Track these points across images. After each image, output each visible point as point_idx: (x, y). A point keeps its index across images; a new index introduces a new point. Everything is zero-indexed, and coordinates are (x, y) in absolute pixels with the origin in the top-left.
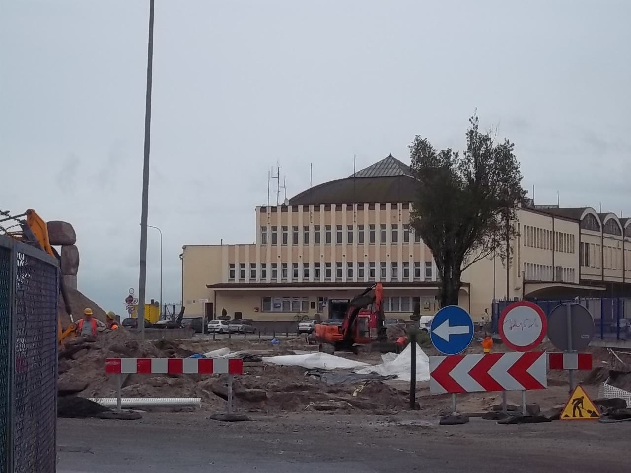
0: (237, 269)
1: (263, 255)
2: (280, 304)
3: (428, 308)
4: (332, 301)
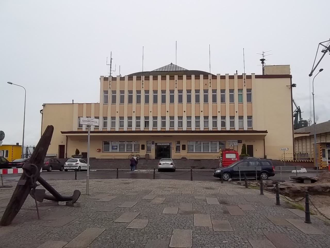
1: (105, 110)
2: (117, 146)
4: (158, 145)
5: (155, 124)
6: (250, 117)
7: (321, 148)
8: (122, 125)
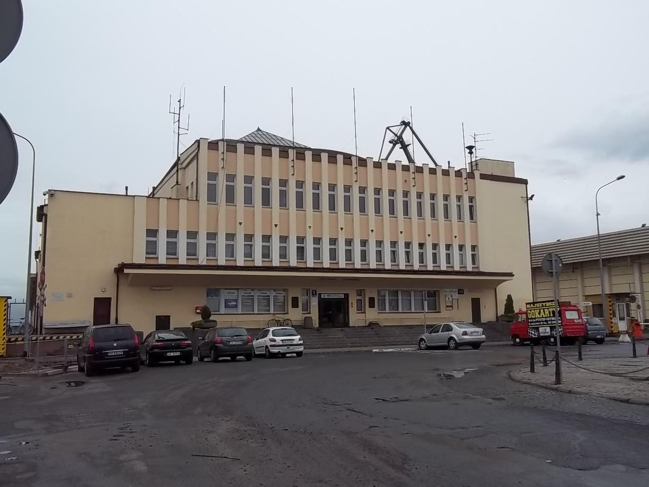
0: (162, 240)
2: (236, 301)
3: (451, 306)
4: (322, 297)
5: (317, 253)
7: (610, 302)
8: (249, 254)
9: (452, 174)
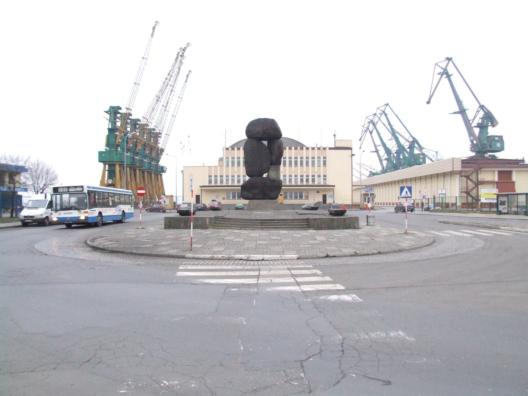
6: (325, 176)
9: (316, 149)
